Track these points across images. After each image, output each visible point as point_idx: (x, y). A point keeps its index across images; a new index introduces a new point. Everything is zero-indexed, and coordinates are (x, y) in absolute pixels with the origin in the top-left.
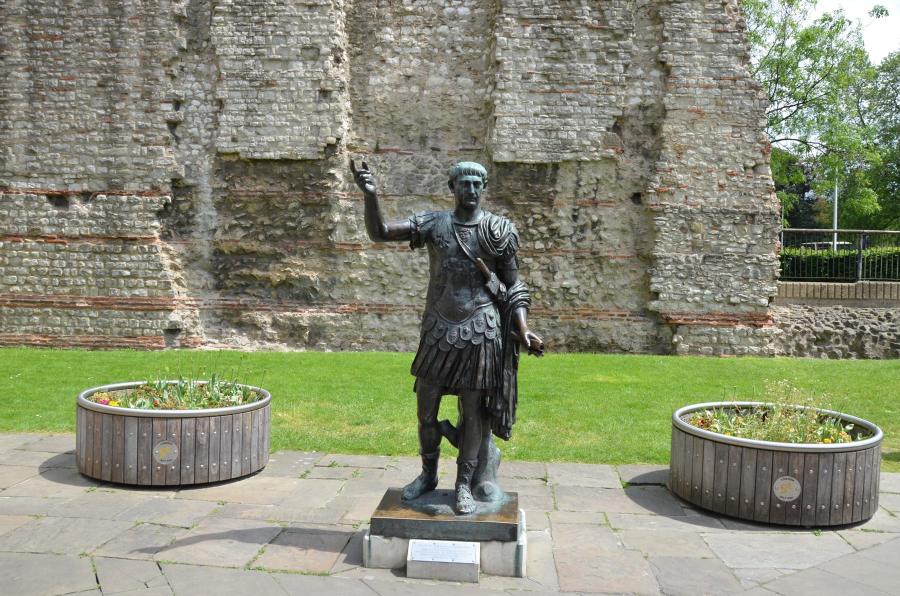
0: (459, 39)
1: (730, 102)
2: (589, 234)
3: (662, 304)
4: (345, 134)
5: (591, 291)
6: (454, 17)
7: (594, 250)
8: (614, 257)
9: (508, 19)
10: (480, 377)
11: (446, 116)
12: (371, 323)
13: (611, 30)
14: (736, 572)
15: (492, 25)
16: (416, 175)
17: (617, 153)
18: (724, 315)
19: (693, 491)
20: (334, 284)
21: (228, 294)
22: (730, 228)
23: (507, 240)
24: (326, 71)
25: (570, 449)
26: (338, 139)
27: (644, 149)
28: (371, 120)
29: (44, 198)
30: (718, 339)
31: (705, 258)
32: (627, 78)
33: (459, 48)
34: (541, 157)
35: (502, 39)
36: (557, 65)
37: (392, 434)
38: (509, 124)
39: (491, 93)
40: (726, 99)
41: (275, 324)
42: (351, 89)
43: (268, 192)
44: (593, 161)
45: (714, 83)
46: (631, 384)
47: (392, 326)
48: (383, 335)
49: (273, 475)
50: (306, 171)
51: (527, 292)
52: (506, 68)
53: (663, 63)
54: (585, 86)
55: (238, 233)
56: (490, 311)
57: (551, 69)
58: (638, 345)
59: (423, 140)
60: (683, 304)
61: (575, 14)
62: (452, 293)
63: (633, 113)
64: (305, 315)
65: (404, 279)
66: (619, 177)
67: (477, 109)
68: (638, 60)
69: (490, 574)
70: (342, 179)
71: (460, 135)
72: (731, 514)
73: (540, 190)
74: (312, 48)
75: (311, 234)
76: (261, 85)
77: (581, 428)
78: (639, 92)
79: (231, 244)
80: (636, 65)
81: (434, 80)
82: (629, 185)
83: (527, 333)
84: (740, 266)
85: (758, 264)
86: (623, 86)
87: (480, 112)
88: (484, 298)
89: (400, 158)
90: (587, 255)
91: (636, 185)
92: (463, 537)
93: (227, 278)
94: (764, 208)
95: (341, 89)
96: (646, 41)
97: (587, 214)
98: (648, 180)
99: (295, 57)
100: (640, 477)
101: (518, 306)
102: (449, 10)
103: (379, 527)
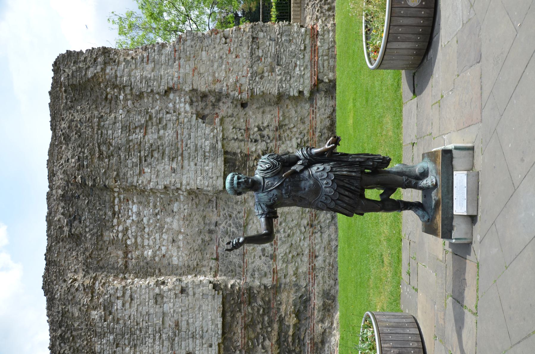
0: (151, 211)
1: (188, 53)
2: (265, 133)
3: (306, 89)
4: (207, 278)
5: (299, 131)
6: (138, 214)
7: (275, 129)
8: (279, 117)
9: (140, 182)
10: (354, 174)
11: (197, 218)
12: (320, 262)
13: (147, 122)
14: (465, 22)
15: (143, 191)
16: (231, 236)
17: (218, 117)
18: (312, 53)
19: (417, 55)
20: (297, 285)
21: (304, 350)
22: (260, 51)
23: (272, 160)
24: (170, 290)
25: (394, 132)
26: (210, 282)
27: (215, 101)
28: (199, 263)
30: (326, 55)
31: (278, 65)
32: (174, 112)
33: (157, 211)
34: (220, 161)
35: (152, 185)
36: (167, 153)
37: (389, 240)
38: (201, 180)
39: (183, 191)
40: (186, 55)
41: (322, 321)
42: (180, 275)
43: (242, 325)
44: (223, 131)
45: (177, 62)
46: (354, 103)
47: (322, 249)
48: (328, 254)
49: (417, 312)
50: (230, 302)
51: (302, 149)
52: (168, 183)
53: (166, 92)
54: (179, 136)
55: (267, 344)
56: (314, 169)
57: (169, 156)
58: (331, 102)
59: (210, 232)
60: (306, 77)
61: (137, 143)
62: (304, 192)
63: (194, 108)
64: (317, 302)
65: (293, 242)
66: (232, 116)
67: (192, 200)
68: (164, 106)
69: (473, 165)
70: (234, 281)
71: (208, 209)
72: (430, 31)
73: (240, 162)
74: (156, 298)
75: (267, 299)
76: (178, 329)
77: (381, 128)
78: (182, 105)
79: (274, 348)
80: (167, 107)
81: (175, 226)
82: (236, 110)
83: (326, 147)
84: (283, 44)
85: (281, 34)
86: (179, 114)
87: (194, 198)
88: (306, 173)
89: (221, 245)
90: (278, 134)
91: (236, 106)
92: (451, 182)
94: (249, 32)
95: (180, 280)
96: (153, 102)
97: (254, 134)
98: (233, 99)
99: (161, 309)
100: (410, 88)
101: (311, 153)
102: (134, 217)
103: (447, 234)
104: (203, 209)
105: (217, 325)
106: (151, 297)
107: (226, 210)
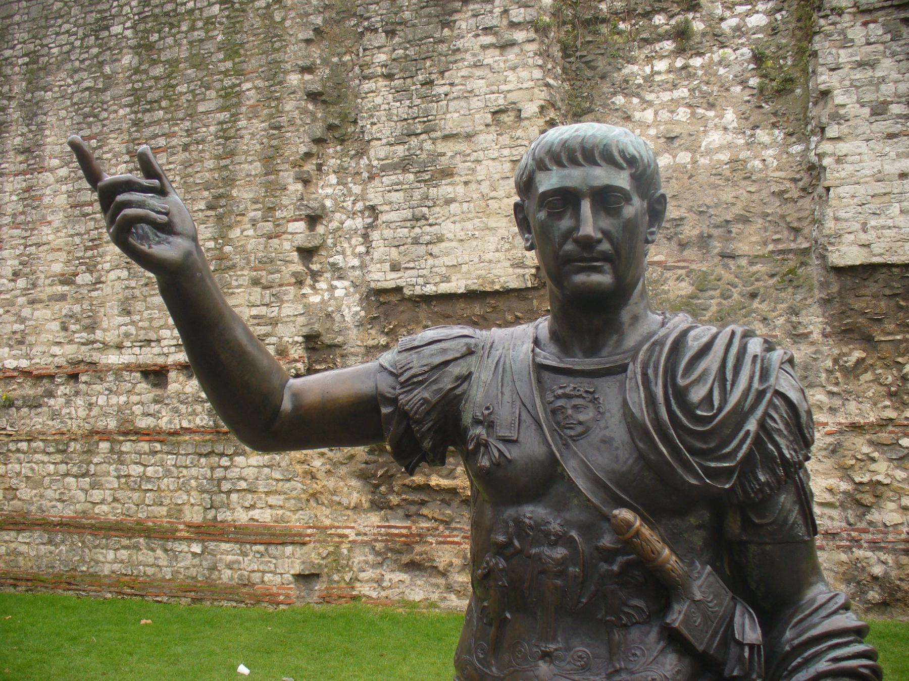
16: (695, 301)
23: (752, 425)
29: (138, 375)
39: (816, 147)
67: (795, 180)
81: (715, 138)
87: (801, 184)
89: (668, 274)
93: (391, 491)
99: (482, 127)
104: (768, 215)
105: (447, 279)
106: (512, 97)
107: (771, 282)
